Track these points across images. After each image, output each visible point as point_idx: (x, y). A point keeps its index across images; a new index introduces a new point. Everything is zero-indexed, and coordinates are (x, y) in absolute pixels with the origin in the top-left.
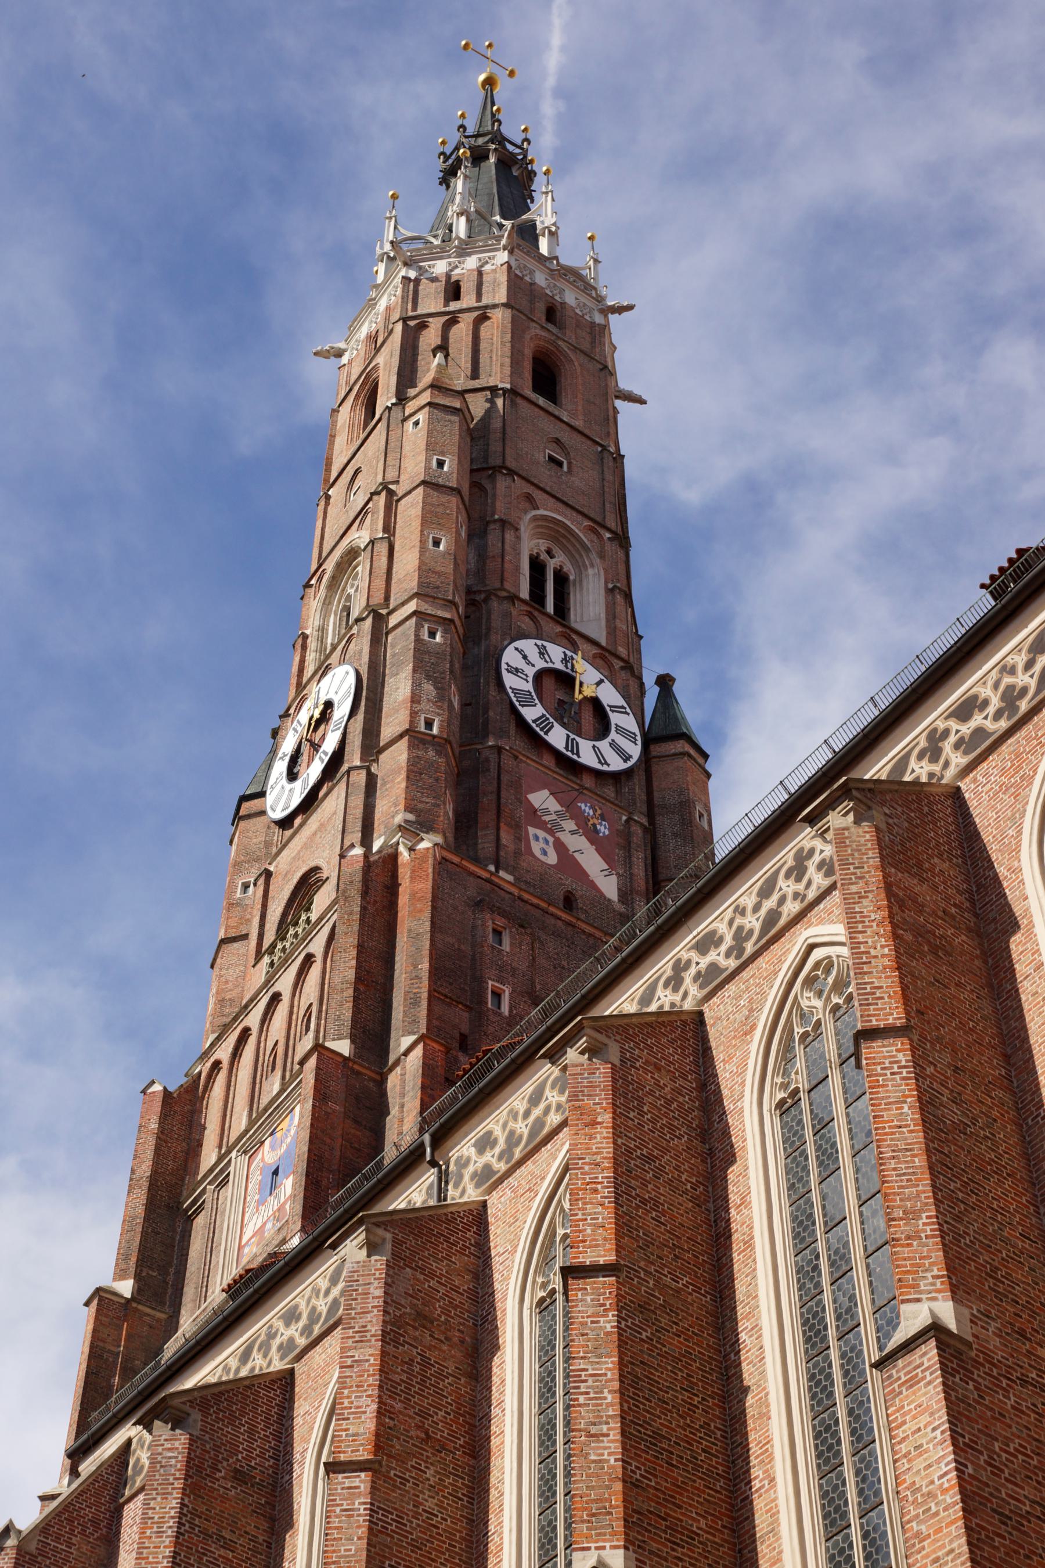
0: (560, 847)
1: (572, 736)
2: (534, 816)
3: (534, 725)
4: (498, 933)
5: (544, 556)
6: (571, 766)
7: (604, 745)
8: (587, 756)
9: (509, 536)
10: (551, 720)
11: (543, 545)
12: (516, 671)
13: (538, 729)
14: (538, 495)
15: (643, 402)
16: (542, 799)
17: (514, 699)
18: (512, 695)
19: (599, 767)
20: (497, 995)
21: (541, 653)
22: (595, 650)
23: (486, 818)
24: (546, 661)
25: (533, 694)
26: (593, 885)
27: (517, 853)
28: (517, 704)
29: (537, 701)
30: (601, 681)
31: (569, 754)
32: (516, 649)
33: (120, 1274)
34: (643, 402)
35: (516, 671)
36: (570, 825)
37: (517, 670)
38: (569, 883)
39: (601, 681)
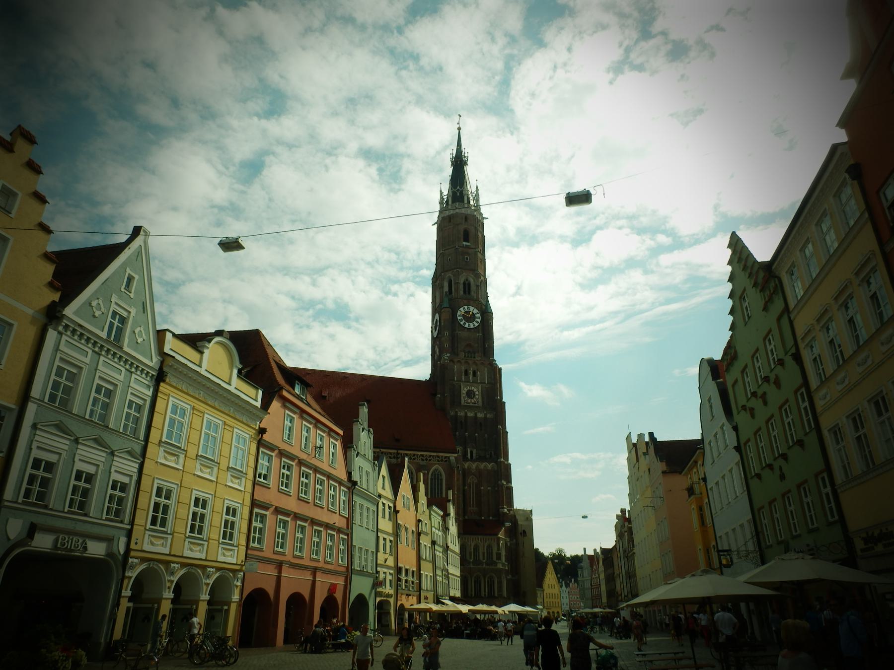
6: (469, 329)
8: (472, 326)
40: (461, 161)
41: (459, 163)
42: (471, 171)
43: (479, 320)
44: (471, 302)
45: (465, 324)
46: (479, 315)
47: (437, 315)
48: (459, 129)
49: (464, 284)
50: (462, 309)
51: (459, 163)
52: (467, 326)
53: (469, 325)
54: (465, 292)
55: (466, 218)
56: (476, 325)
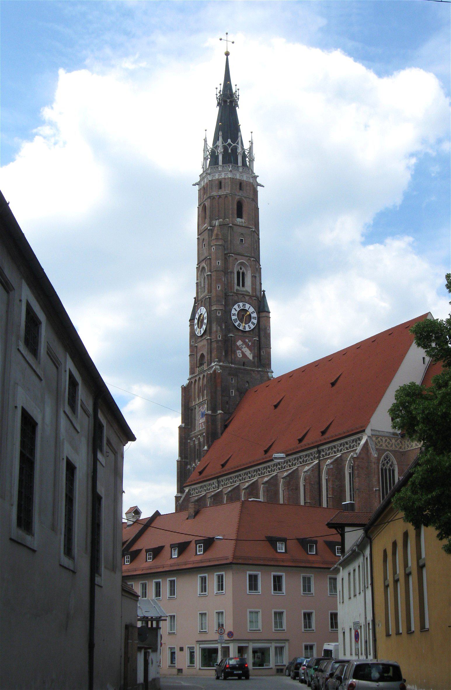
0: (243, 353)
2: (238, 348)
4: (232, 379)
5: (240, 270)
7: (250, 324)
8: (247, 329)
9: (232, 275)
11: (239, 267)
12: (234, 315)
14: (238, 257)
15: (263, 187)
16: (239, 343)
20: (232, 392)
22: (249, 297)
23: (230, 353)
26: (248, 358)
27: (235, 358)
33: (182, 423)
34: (263, 187)
35: (234, 315)
36: (244, 346)
38: (244, 360)
40: (231, 102)
41: (228, 102)
42: (241, 113)
43: (255, 321)
44: (247, 298)
46: (255, 315)
47: (203, 310)
48: (227, 54)
49: (238, 273)
50: (236, 306)
51: (228, 102)
52: (241, 328)
54: (238, 285)
55: (241, 185)
56: (252, 327)
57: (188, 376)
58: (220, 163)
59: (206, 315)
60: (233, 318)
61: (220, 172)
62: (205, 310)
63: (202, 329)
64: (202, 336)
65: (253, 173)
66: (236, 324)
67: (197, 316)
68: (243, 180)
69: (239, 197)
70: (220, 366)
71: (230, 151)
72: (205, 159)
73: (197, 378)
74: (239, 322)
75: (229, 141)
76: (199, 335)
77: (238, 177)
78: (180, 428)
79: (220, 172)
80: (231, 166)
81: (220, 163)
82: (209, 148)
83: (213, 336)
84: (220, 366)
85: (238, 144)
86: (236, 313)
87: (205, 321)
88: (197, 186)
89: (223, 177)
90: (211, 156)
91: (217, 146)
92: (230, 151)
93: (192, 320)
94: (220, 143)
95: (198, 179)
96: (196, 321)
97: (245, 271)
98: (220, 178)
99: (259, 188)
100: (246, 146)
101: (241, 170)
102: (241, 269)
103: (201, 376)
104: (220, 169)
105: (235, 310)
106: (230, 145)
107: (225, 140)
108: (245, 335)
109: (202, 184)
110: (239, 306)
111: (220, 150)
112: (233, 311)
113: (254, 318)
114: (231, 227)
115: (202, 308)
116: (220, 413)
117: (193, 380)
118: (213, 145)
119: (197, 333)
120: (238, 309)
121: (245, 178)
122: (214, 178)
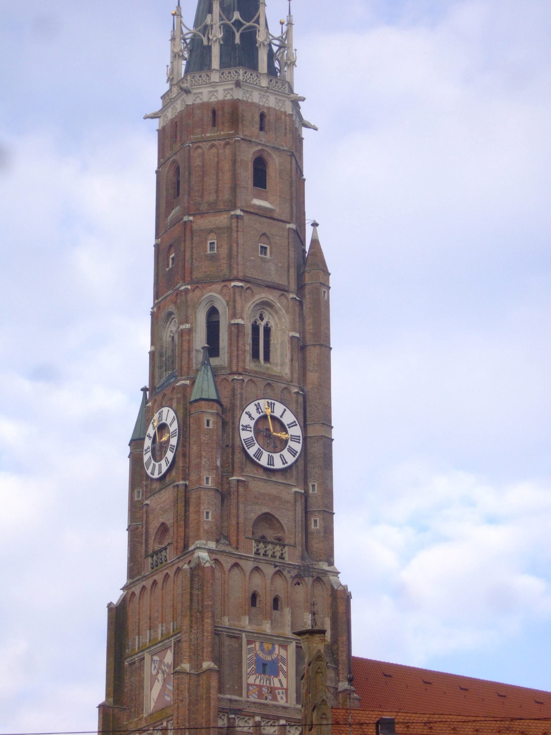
1: (271, 454)
3: (254, 458)
7: (285, 452)
8: (278, 464)
10: (262, 450)
12: (246, 428)
13: (255, 459)
15: (316, 129)
17: (245, 446)
18: (244, 444)
19: (283, 466)
21: (257, 409)
24: (260, 413)
25: (254, 438)
28: (246, 448)
29: (255, 442)
30: (285, 410)
31: (269, 466)
32: (246, 413)
33: (107, 695)
35: (246, 428)
37: (246, 427)
39: (285, 410)
43: (298, 447)
45: (259, 454)
46: (296, 431)
47: (168, 415)
49: (255, 328)
50: (251, 408)
52: (264, 461)
53: (271, 460)
56: (290, 459)
57: (123, 579)
58: (215, 63)
59: (174, 427)
60: (245, 435)
61: (214, 85)
62: (172, 414)
63: (163, 462)
64: (162, 478)
65: (291, 91)
66: (251, 452)
67: (151, 431)
68: (269, 108)
69: (260, 148)
70: (210, 551)
71: (237, 41)
72: (176, 56)
73: (148, 583)
74: (257, 446)
75: (237, 15)
76: (156, 476)
77: (256, 97)
78: (102, 707)
79: (214, 85)
80: (241, 72)
81: (215, 63)
82: (185, 31)
83: (193, 477)
84: (210, 551)
85: (257, 22)
86: (252, 423)
87: (174, 441)
88: (157, 120)
89: (221, 97)
90: (191, 52)
91: (206, 27)
92: (237, 41)
93: (136, 443)
94: (215, 17)
95: (158, 105)
96: (148, 443)
97: (272, 324)
98: (213, 99)
99: (305, 132)
100: (275, 30)
101: (264, 83)
102: (262, 319)
103: (159, 577)
104: (215, 77)
105: (247, 419)
106: (238, 24)
107: (226, 11)
108: (274, 479)
109: (170, 114)
110: (258, 407)
111: (218, 34)
112: (245, 420)
113: (295, 439)
114: (238, 217)
115: (165, 410)
116: (210, 670)
117: (137, 592)
118: (196, 26)
119: (149, 472)
120: (256, 416)
121: (271, 102)
122: (198, 101)
